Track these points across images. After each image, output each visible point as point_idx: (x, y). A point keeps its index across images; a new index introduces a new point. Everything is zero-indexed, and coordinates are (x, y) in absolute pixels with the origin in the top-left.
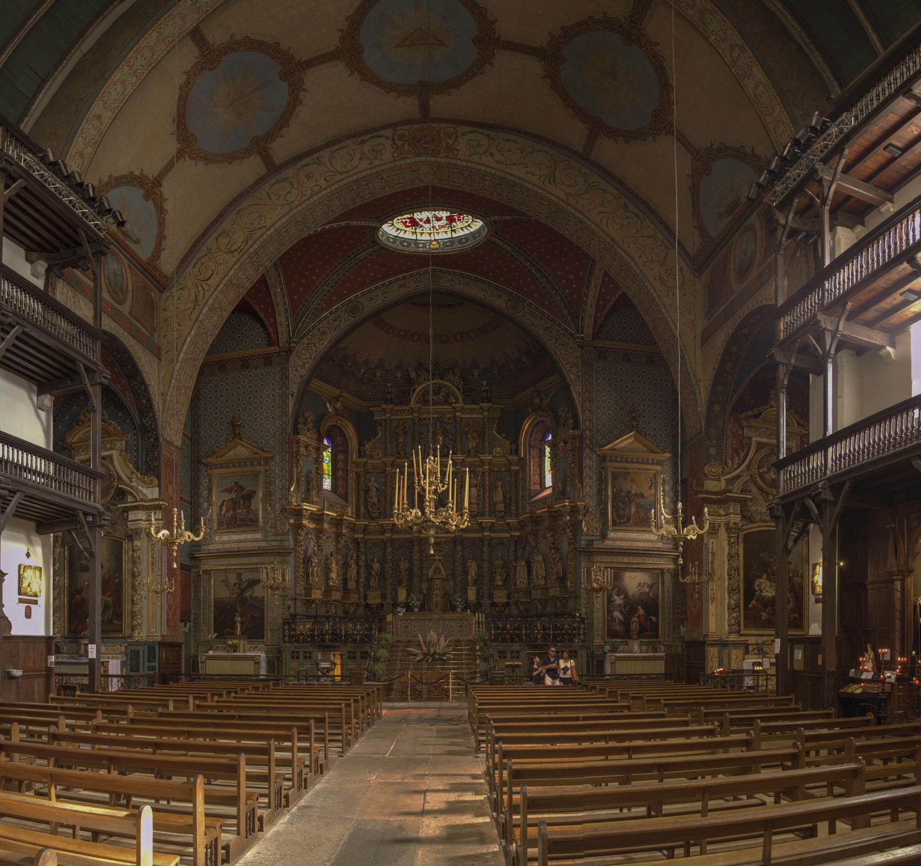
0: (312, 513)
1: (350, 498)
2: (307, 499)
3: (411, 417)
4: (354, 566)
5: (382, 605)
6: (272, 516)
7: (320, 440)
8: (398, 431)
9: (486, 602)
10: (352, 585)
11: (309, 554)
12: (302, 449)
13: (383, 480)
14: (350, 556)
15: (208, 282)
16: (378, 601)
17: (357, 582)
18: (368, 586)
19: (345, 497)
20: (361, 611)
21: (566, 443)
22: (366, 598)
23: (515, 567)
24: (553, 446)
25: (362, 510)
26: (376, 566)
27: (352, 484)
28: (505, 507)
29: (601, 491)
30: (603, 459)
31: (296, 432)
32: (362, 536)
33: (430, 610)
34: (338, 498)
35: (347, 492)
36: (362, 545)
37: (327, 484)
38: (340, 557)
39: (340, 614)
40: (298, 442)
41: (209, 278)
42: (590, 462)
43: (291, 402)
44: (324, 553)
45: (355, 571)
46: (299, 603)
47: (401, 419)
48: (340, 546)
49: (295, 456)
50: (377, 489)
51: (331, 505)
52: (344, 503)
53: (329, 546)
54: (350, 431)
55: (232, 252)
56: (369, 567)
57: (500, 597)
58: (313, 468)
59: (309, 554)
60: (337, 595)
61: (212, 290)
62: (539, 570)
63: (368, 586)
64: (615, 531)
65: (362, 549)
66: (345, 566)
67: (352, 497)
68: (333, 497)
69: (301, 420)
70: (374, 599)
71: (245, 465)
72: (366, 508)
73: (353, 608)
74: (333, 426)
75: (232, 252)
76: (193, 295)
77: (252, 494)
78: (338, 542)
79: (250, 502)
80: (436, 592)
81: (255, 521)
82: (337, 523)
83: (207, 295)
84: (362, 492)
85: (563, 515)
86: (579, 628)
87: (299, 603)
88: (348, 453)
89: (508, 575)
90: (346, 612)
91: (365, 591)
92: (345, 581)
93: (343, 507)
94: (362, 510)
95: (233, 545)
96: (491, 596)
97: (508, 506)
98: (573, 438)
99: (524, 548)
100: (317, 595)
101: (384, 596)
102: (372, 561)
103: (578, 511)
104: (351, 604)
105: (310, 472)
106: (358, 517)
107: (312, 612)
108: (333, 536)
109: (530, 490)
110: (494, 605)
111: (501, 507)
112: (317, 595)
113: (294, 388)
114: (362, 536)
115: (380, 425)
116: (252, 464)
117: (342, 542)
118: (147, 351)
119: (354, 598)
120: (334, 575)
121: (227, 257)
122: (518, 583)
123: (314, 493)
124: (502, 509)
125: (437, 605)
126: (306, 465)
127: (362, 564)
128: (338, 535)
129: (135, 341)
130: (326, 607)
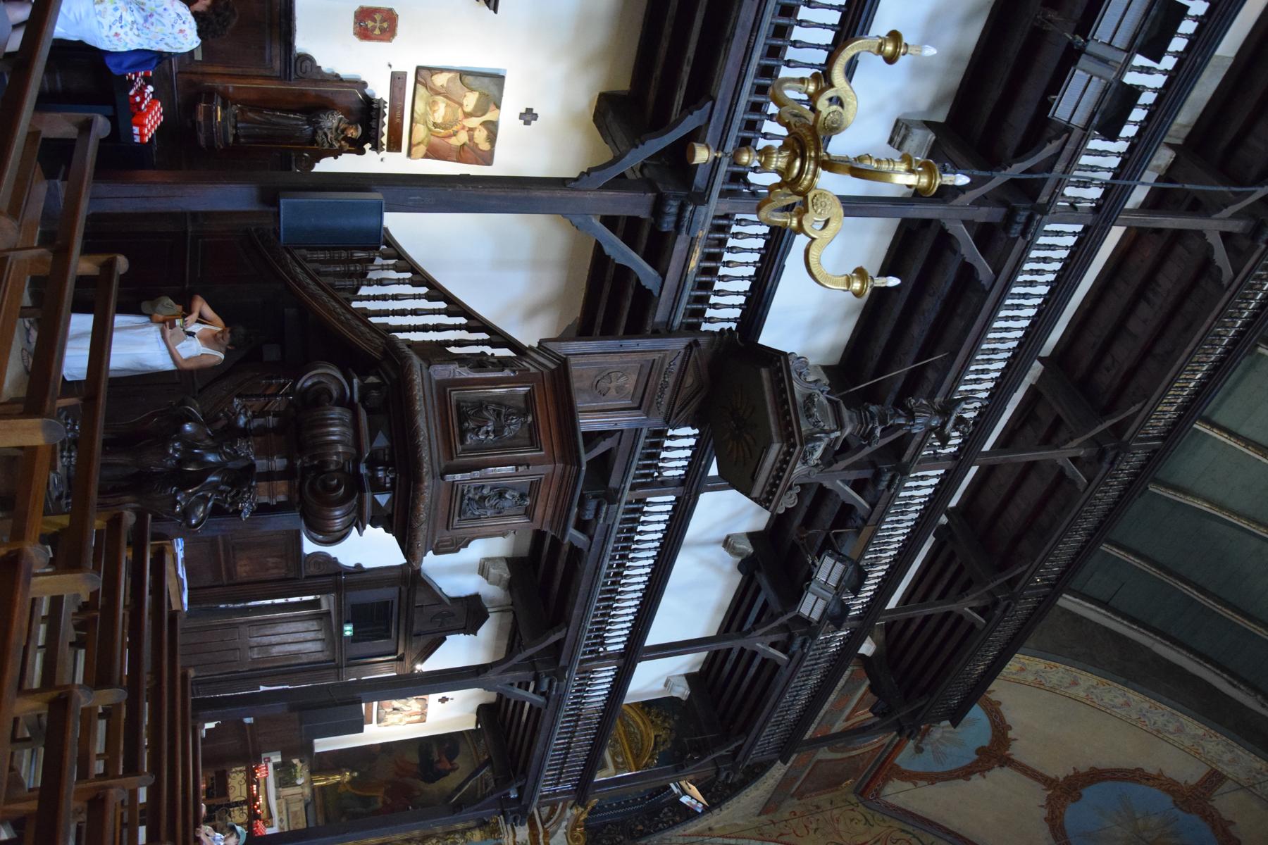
118: (769, 796)
129: (780, 777)
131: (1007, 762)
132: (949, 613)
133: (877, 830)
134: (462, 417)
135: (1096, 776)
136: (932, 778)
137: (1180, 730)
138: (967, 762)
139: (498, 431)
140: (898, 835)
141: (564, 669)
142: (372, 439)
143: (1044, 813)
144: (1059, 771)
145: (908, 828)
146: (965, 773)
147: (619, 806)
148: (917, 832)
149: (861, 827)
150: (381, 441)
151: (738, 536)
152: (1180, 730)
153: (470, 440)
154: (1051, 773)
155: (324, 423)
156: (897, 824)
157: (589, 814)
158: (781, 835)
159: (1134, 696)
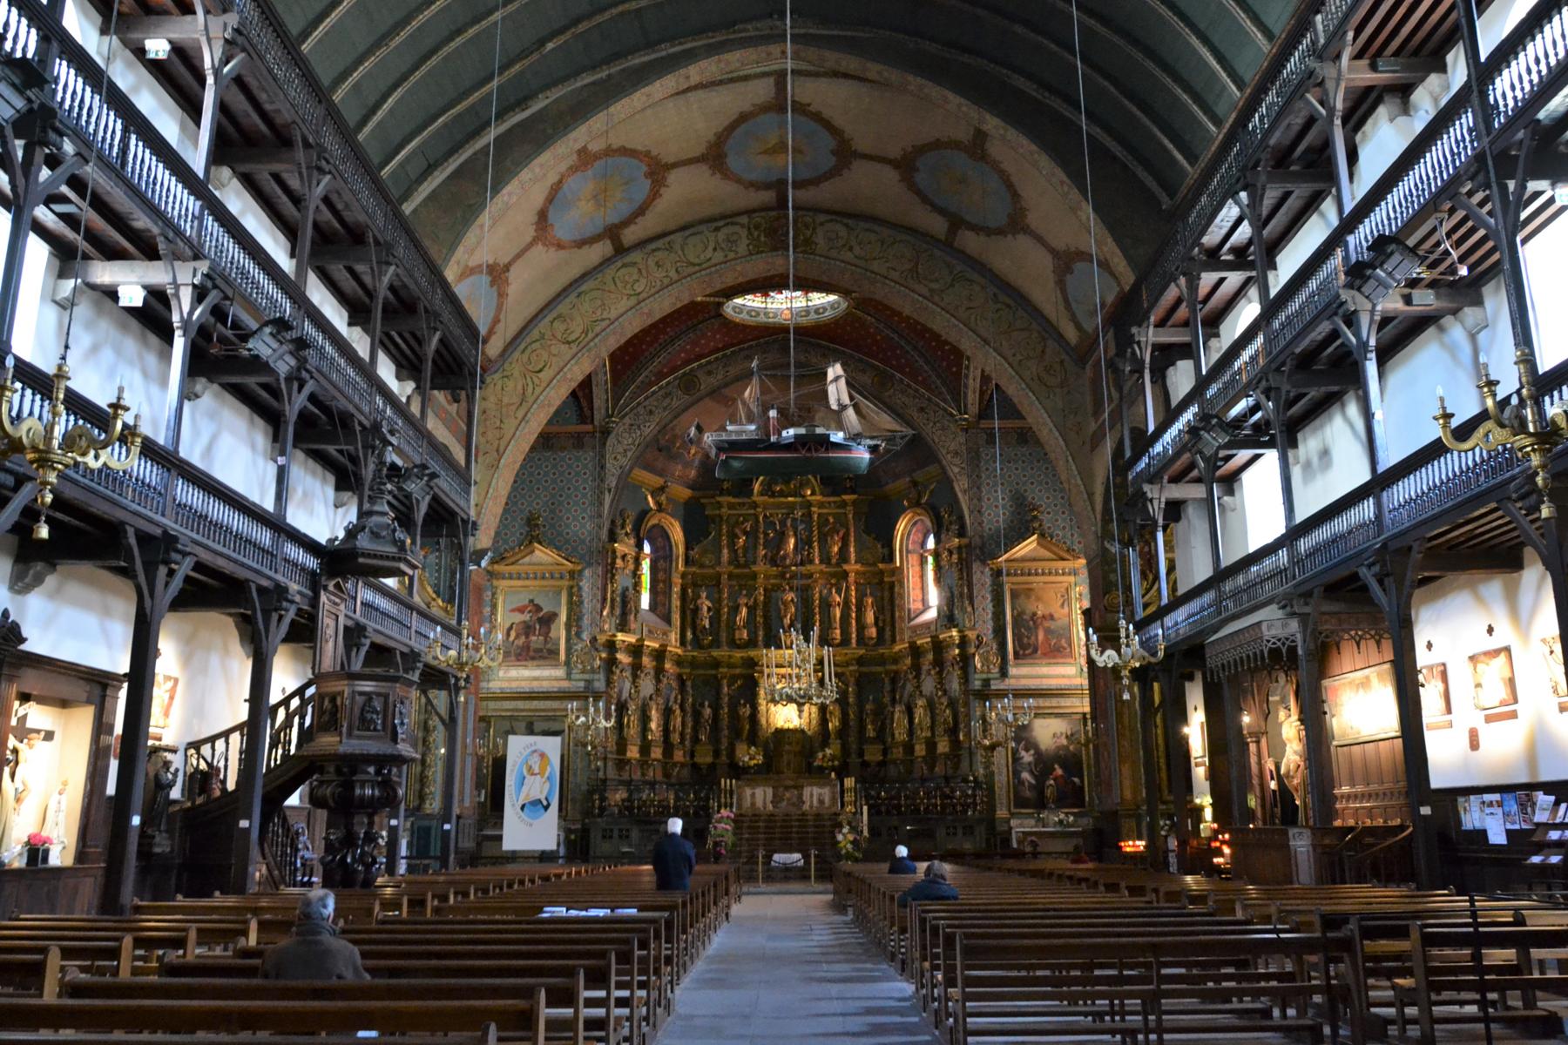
0: (630, 644)
1: (673, 620)
2: (623, 627)
3: (752, 511)
4: (678, 712)
5: (712, 766)
6: (579, 647)
7: (640, 546)
8: (737, 531)
9: (854, 760)
10: (675, 738)
11: (623, 698)
12: (619, 562)
13: (716, 596)
14: (672, 699)
15: (540, 375)
16: (709, 759)
17: (682, 735)
18: (696, 740)
19: (667, 620)
20: (686, 772)
21: (951, 553)
22: (692, 756)
23: (893, 713)
24: (937, 554)
25: (689, 635)
26: (708, 712)
27: (676, 602)
28: (878, 633)
29: (999, 615)
30: (997, 573)
31: (613, 538)
32: (688, 670)
33: (779, 772)
34: (658, 620)
35: (670, 612)
36: (689, 683)
37: (645, 602)
38: (661, 701)
39: (659, 777)
40: (614, 551)
41: (540, 371)
42: (982, 577)
43: (608, 499)
44: (642, 695)
45: (679, 720)
46: (610, 764)
47: (740, 515)
48: (662, 686)
49: (610, 572)
50: (709, 609)
51: (650, 631)
52: (666, 627)
53: (647, 686)
54: (677, 534)
55: (569, 343)
56: (697, 715)
57: (873, 754)
58: (629, 582)
59: (623, 698)
60: (657, 753)
61: (544, 385)
62: (919, 713)
63: (696, 740)
64: (1016, 665)
65: (689, 689)
66: (667, 713)
67: (676, 618)
68: (653, 618)
69: (619, 522)
70: (704, 758)
71: (543, 578)
72: (694, 633)
73: (677, 770)
74: (654, 526)
75: (569, 343)
76: (520, 387)
77: (552, 617)
78: (658, 681)
79: (549, 629)
80: (787, 747)
81: (554, 653)
82: (659, 655)
83: (538, 391)
84: (688, 612)
85: (948, 646)
86: (974, 796)
87: (610, 764)
88: (671, 561)
89: (883, 723)
90: (667, 775)
91: (693, 747)
92: (666, 731)
93: (665, 634)
94: (689, 635)
95: (523, 684)
96: (861, 754)
97: (880, 632)
98: (960, 548)
99: (904, 687)
100: (633, 753)
101: (717, 753)
102: (702, 705)
103: (970, 641)
104: (675, 764)
105: (627, 589)
106: (683, 643)
107: (626, 776)
108: (652, 672)
109: (909, 610)
110: (865, 764)
111: (873, 632)
112: (633, 753)
113: (612, 481)
114: (688, 670)
115: (714, 522)
116: (552, 577)
117: (665, 681)
119: (679, 756)
120: (653, 725)
121: (564, 347)
122: (897, 735)
123: (632, 617)
124: (874, 635)
125: (789, 764)
126: (623, 580)
127: (689, 709)
128: (659, 671)
130: (642, 767)
131: (507, 267)
132: (434, 361)
133: (516, 373)
134: (369, 730)
135: (542, 216)
136: (496, 321)
137: (542, 166)
138: (495, 294)
139: (377, 713)
140: (525, 357)
141: (412, 651)
142: (369, 773)
143: (552, 250)
144: (530, 233)
145: (522, 346)
146: (502, 295)
147: (438, 571)
148: (528, 340)
149: (511, 384)
150: (371, 770)
151: (336, 498)
152: (542, 166)
153: (379, 727)
154: (529, 239)
155: (362, 797)
156: (516, 354)
157: (438, 596)
158: (497, 451)
159: (505, 191)
